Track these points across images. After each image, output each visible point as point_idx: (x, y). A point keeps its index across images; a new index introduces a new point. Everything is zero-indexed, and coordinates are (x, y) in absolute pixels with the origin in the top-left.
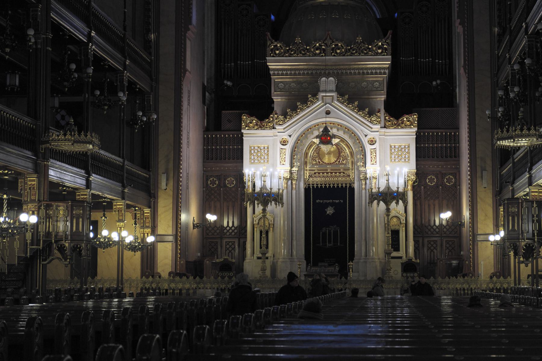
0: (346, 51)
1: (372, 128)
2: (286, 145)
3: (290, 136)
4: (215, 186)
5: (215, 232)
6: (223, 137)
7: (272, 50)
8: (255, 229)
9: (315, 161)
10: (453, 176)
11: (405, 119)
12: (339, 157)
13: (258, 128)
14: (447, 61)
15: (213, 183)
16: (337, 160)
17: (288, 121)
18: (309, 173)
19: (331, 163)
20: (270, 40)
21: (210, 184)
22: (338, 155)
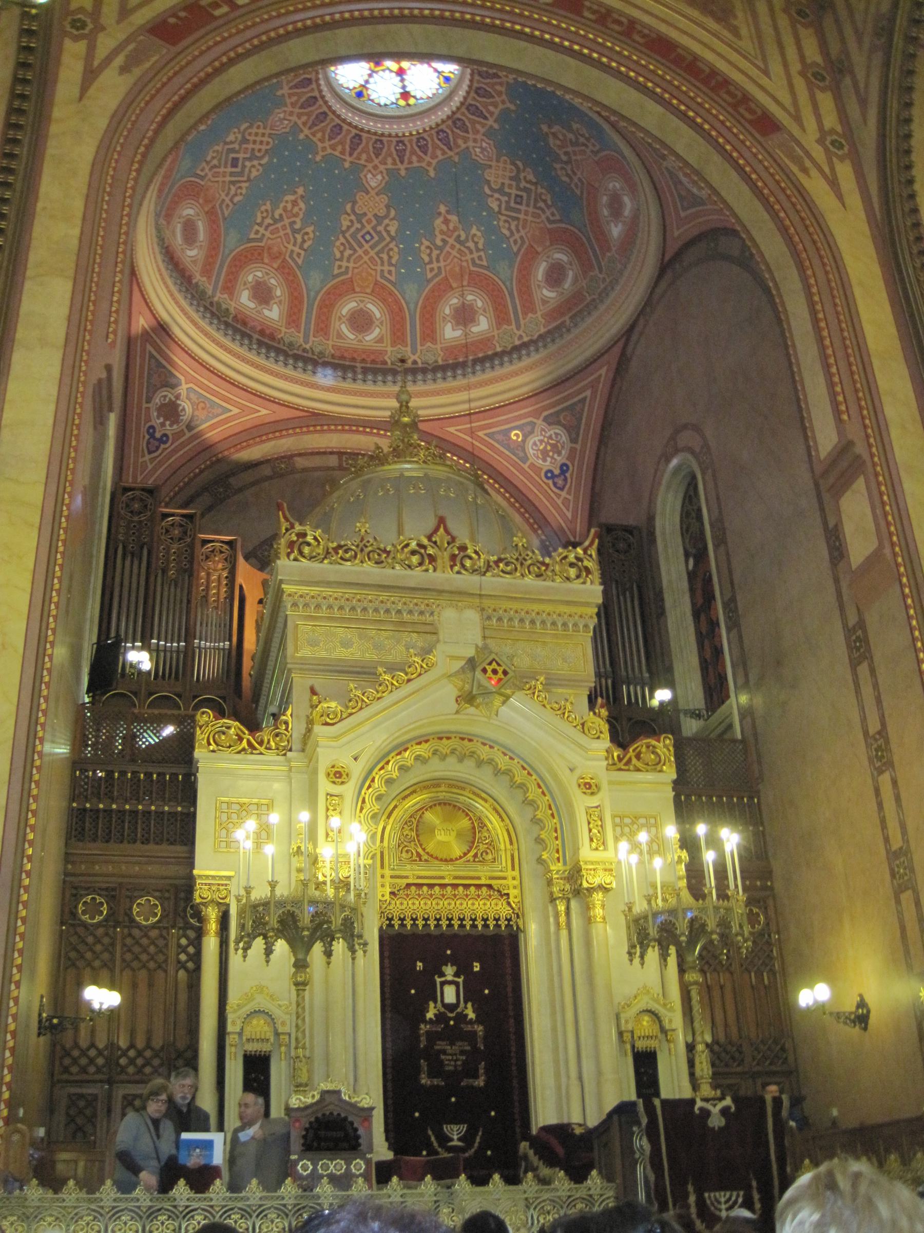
0: (489, 566)
1: (586, 750)
2: (343, 783)
3: (356, 759)
4: (98, 919)
5: (92, 1061)
6: (131, 779)
7: (291, 544)
8: (229, 1051)
9: (407, 852)
10: (760, 908)
11: (644, 749)
12: (473, 842)
13: (244, 749)
14: (646, 675)
15: (94, 909)
16: (469, 851)
17: (351, 714)
18: (393, 885)
19: (451, 860)
20: (287, 520)
21: (84, 913)
22: (471, 839)
